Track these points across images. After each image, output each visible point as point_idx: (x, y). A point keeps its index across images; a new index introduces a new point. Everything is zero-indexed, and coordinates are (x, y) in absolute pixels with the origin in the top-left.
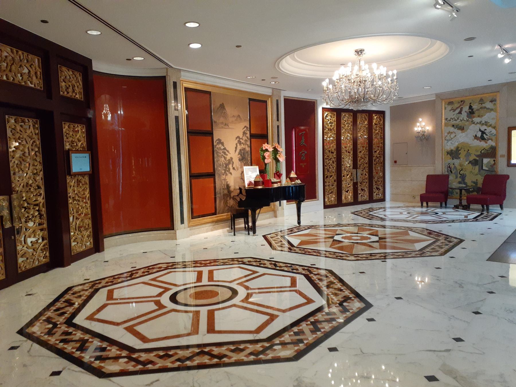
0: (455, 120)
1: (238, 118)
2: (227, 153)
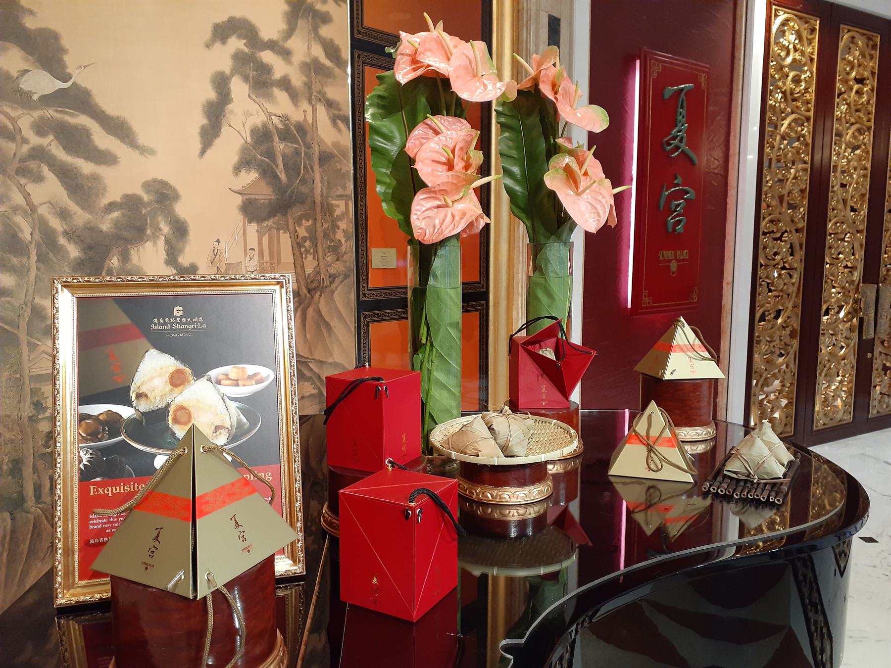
2: (102, 139)
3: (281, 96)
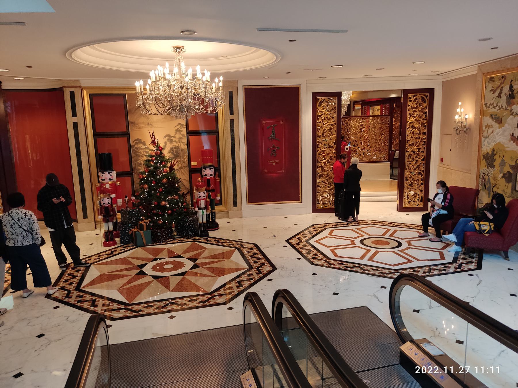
0: (494, 107)
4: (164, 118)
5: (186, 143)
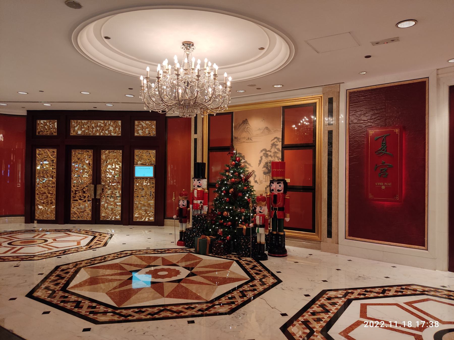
1: (266, 130)
3: (270, 157)
4: (262, 133)
5: (281, 157)
